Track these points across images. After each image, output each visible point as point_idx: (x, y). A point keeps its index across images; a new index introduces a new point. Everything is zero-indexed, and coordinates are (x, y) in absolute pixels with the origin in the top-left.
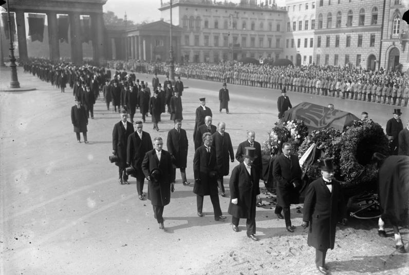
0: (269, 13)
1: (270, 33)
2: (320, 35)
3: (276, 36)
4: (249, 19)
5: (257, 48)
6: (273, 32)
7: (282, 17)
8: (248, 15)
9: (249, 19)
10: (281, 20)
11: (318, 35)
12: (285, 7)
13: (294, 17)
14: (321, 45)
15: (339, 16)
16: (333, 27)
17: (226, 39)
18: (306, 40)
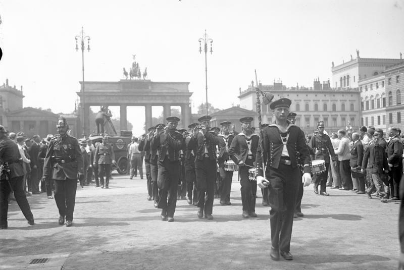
0: (341, 95)
1: (344, 113)
2: (399, 111)
3: (350, 115)
4: (321, 100)
5: (331, 127)
6: (347, 111)
7: (355, 97)
8: (321, 97)
9: (321, 100)
10: (355, 101)
11: (389, 112)
12: (358, 88)
13: (367, 97)
14: (393, 121)
15: (390, 96)
16: (394, 105)
17: (316, 119)
18: (379, 117)
